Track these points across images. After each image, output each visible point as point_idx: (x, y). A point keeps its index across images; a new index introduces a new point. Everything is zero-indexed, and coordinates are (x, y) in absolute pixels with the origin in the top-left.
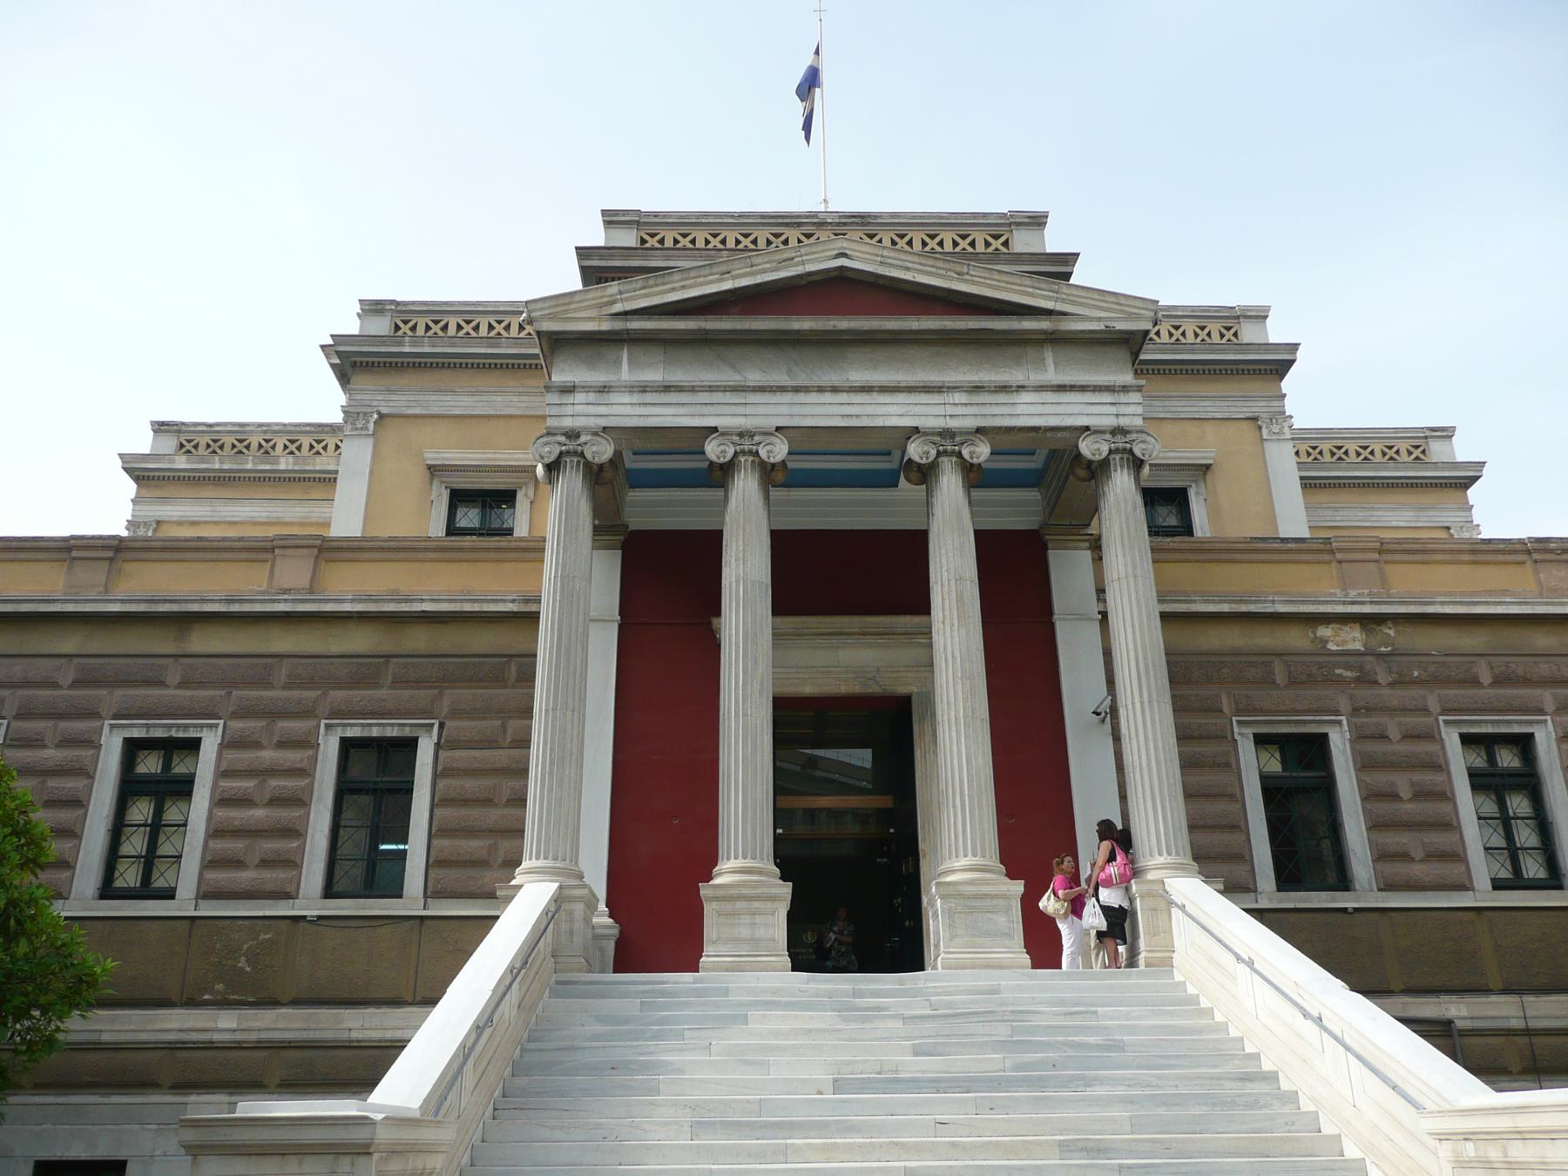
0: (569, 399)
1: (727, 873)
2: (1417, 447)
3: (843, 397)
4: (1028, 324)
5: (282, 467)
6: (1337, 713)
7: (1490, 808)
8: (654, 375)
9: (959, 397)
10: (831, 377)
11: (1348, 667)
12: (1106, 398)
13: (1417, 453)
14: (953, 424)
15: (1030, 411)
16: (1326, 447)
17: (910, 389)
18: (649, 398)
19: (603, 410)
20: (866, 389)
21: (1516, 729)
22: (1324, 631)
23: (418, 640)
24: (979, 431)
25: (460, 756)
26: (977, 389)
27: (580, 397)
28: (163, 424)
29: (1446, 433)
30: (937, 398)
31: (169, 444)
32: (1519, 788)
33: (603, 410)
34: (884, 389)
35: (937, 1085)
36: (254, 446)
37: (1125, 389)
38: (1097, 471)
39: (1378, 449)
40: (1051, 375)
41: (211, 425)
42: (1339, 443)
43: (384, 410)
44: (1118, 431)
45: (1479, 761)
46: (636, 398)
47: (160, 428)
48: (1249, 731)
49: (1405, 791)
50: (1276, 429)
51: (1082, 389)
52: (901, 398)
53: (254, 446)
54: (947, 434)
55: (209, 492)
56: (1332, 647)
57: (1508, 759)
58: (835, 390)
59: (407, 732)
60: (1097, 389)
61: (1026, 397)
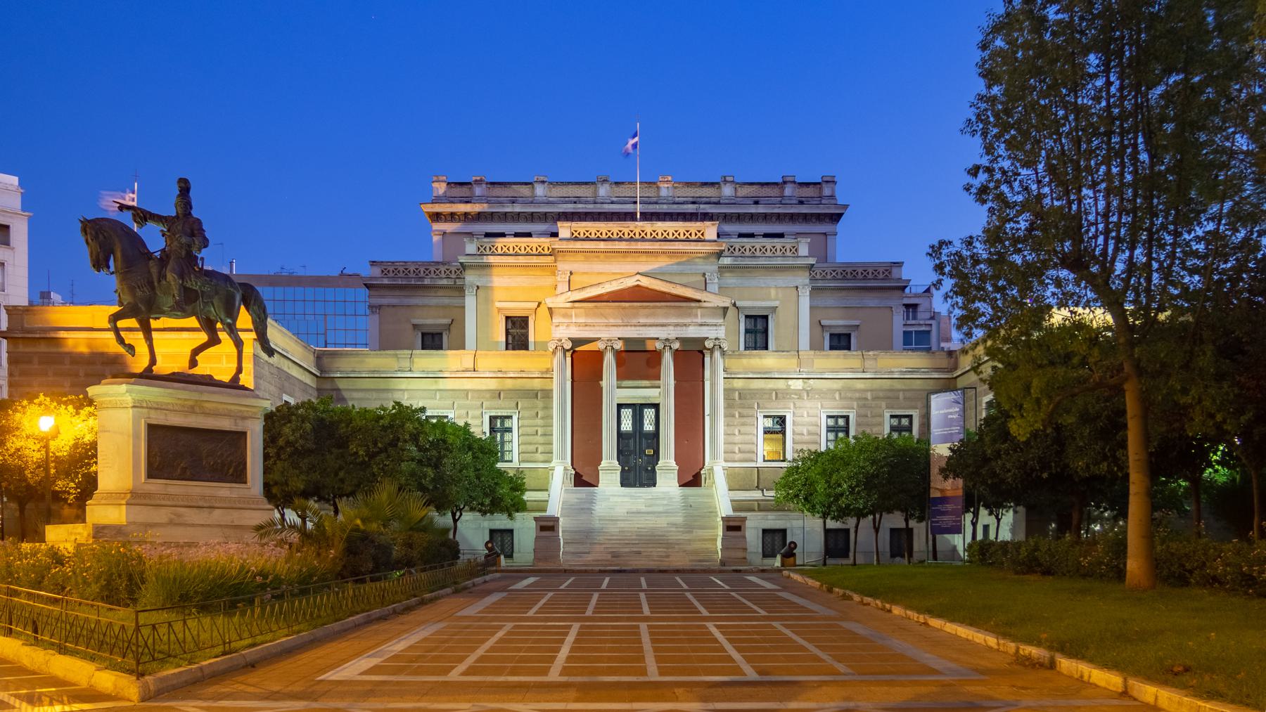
0: (558, 328)
1: (604, 463)
2: (887, 270)
3: (638, 328)
4: (693, 304)
5: (426, 283)
6: (790, 409)
7: (831, 436)
8: (582, 320)
9: (671, 328)
10: (634, 321)
11: (796, 395)
12: (715, 328)
13: (886, 273)
14: (670, 337)
15: (692, 332)
16: (849, 270)
17: (657, 326)
18: (581, 328)
19: (568, 332)
20: (645, 326)
21: (845, 414)
22: (790, 382)
23: (509, 384)
24: (677, 338)
25: (526, 422)
26: (677, 325)
27: (561, 328)
28: (374, 262)
29: (899, 265)
30: (664, 328)
31: (376, 271)
32: (842, 431)
33: (568, 332)
34: (650, 326)
35: (648, 513)
36: (412, 271)
37: (720, 325)
38: (712, 350)
39: (870, 270)
40: (699, 320)
41: (393, 263)
42: (855, 269)
43: (479, 285)
44: (716, 339)
45: (831, 422)
46: (577, 329)
47: (373, 263)
48: (762, 415)
49: (805, 433)
50: (804, 291)
51: (708, 325)
52: (654, 328)
53: (412, 271)
54: (667, 340)
55: (397, 293)
56: (792, 387)
57: (841, 422)
58: (635, 326)
59: (509, 414)
60: (712, 325)
61: (691, 328)
